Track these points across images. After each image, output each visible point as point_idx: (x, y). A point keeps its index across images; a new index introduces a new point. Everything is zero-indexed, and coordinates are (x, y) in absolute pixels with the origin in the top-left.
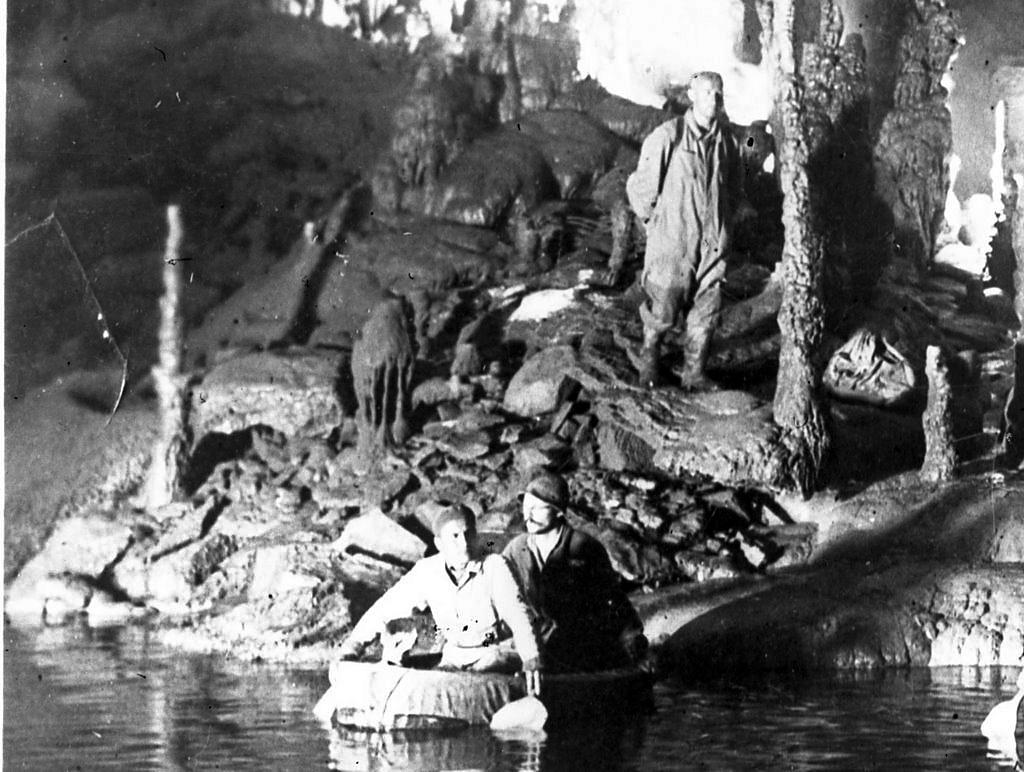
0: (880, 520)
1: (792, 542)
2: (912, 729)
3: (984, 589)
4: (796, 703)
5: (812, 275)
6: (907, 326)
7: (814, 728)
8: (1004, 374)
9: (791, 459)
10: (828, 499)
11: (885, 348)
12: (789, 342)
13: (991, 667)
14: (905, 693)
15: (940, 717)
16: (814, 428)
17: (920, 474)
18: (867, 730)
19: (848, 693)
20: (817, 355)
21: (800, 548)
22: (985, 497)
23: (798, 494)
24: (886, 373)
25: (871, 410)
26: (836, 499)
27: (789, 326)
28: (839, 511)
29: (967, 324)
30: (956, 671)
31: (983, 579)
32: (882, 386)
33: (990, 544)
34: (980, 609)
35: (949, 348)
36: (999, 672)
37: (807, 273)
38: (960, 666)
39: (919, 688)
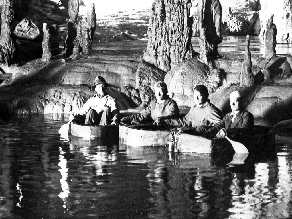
0: (30, 72)
1: (5, 79)
2: (39, 132)
3: (59, 92)
4: (6, 124)
5: (11, 3)
6: (38, 17)
7: (11, 131)
8: (65, 31)
9: (4, 55)
10: (15, 66)
11: (31, 24)
12: (4, 22)
13: (62, 114)
14: (37, 121)
15: (47, 128)
16: (11, 46)
17: (41, 59)
18: (26, 132)
19: (21, 122)
20: (12, 26)
21: (7, 80)
22: (60, 66)
23: (7, 65)
24: (32, 31)
25: (27, 41)
26: (17, 66)
27: (4, 17)
28: (18, 70)
29: (55, 17)
30: (51, 115)
31: (59, 89)
32: (30, 34)
33: (61, 79)
34: (58, 98)
35: (49, 23)
36: (64, 115)
37: (9, 2)
38: (53, 114)
39: (41, 120)
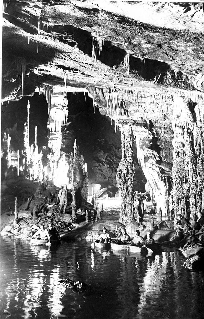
19: (79, 242)
20: (76, 211)
29: (90, 208)
